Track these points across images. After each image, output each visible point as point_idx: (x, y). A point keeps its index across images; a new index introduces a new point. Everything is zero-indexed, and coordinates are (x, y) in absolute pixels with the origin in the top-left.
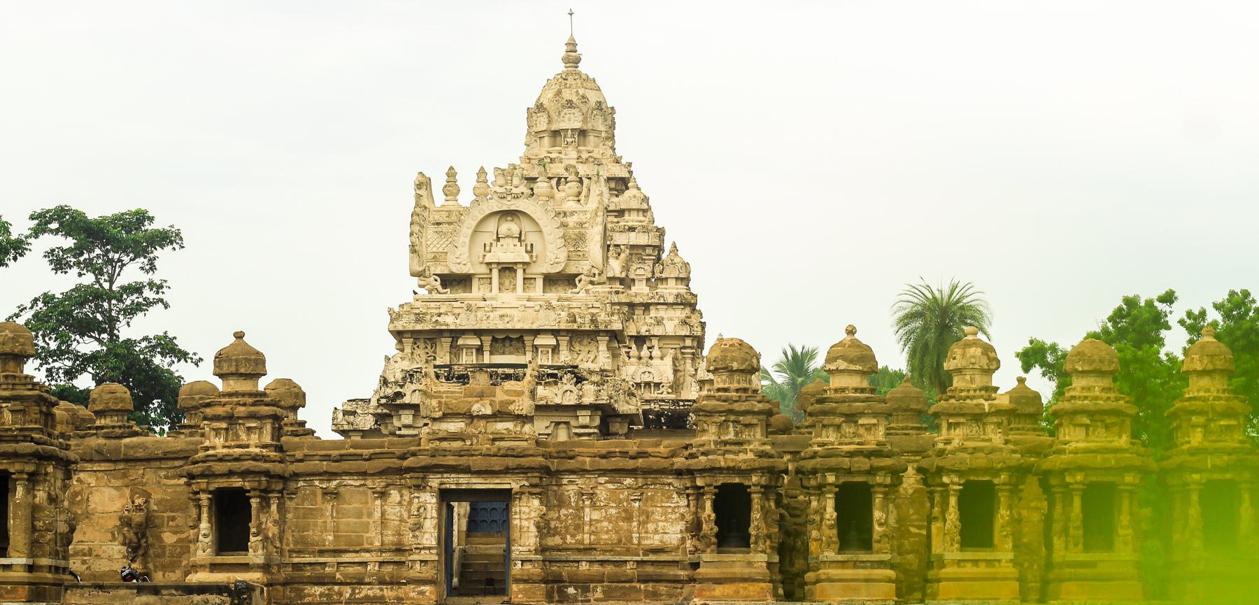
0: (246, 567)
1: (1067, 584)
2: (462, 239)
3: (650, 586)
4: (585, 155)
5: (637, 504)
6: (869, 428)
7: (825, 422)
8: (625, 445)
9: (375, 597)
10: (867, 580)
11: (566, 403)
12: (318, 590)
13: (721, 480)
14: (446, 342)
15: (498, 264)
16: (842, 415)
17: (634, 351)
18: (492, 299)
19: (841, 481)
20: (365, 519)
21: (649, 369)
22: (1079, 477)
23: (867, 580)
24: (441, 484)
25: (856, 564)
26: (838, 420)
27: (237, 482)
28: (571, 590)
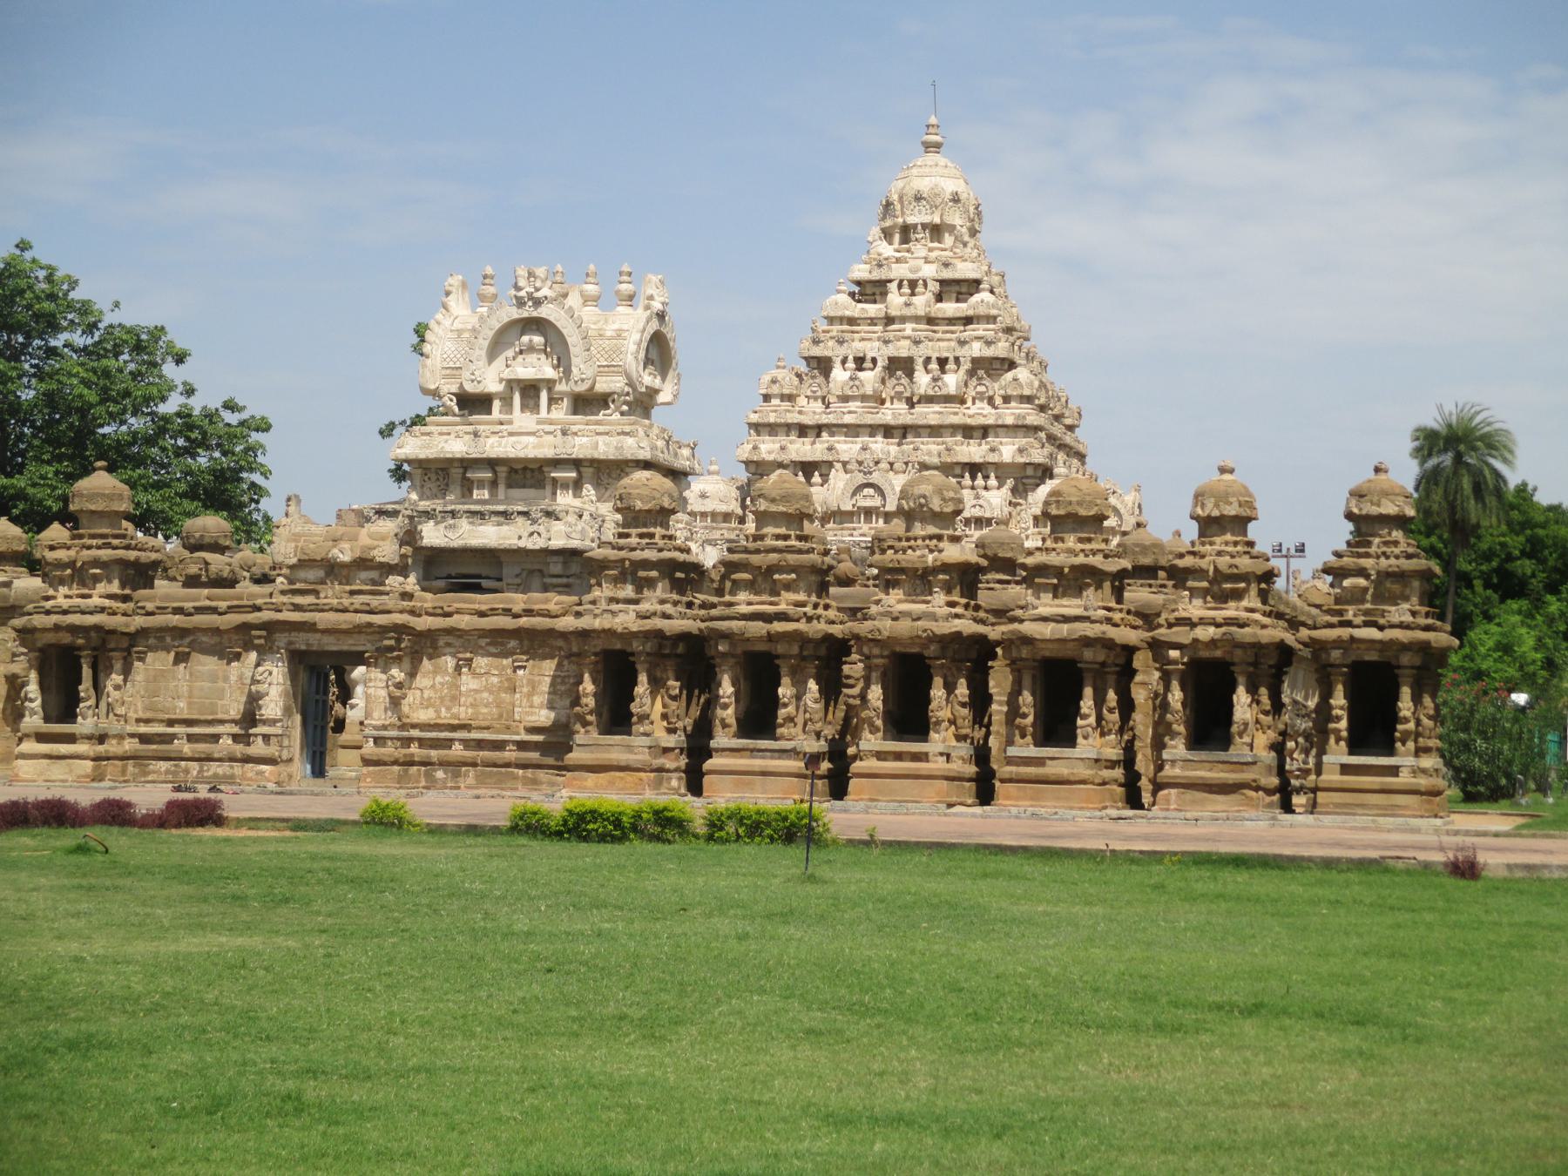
0: (71, 739)
2: (478, 352)
3: (529, 773)
4: (934, 255)
5: (520, 672)
6: (788, 587)
8: (511, 601)
9: (225, 776)
10: (764, 774)
11: (530, 546)
12: (163, 766)
13: (599, 645)
14: (456, 472)
15: (519, 381)
17: (967, 481)
18: (510, 422)
20: (221, 684)
21: (981, 502)
23: (764, 774)
24: (290, 643)
25: (753, 751)
26: (746, 576)
27: (66, 639)
28: (440, 774)
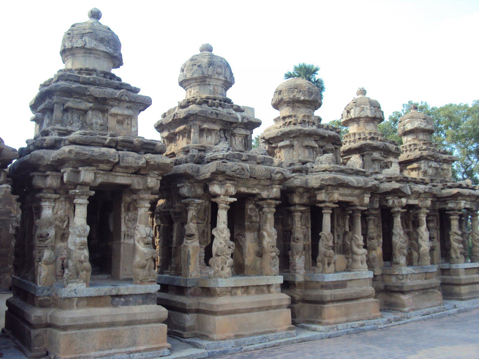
1: (330, 305)
7: (69, 104)
16: (96, 100)
19: (99, 180)
22: (336, 196)
25: (116, 299)
26: (85, 105)
